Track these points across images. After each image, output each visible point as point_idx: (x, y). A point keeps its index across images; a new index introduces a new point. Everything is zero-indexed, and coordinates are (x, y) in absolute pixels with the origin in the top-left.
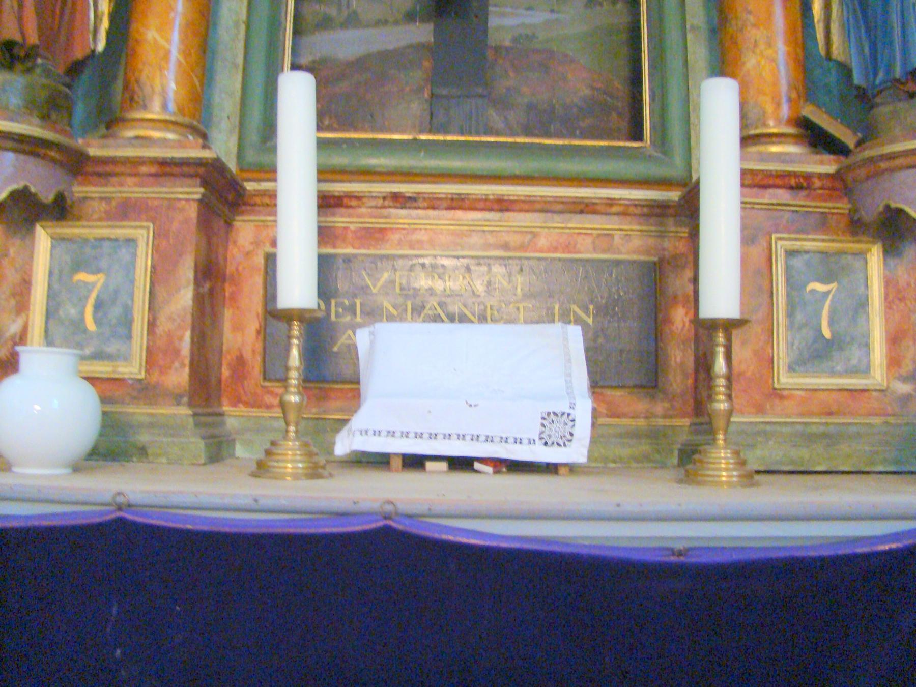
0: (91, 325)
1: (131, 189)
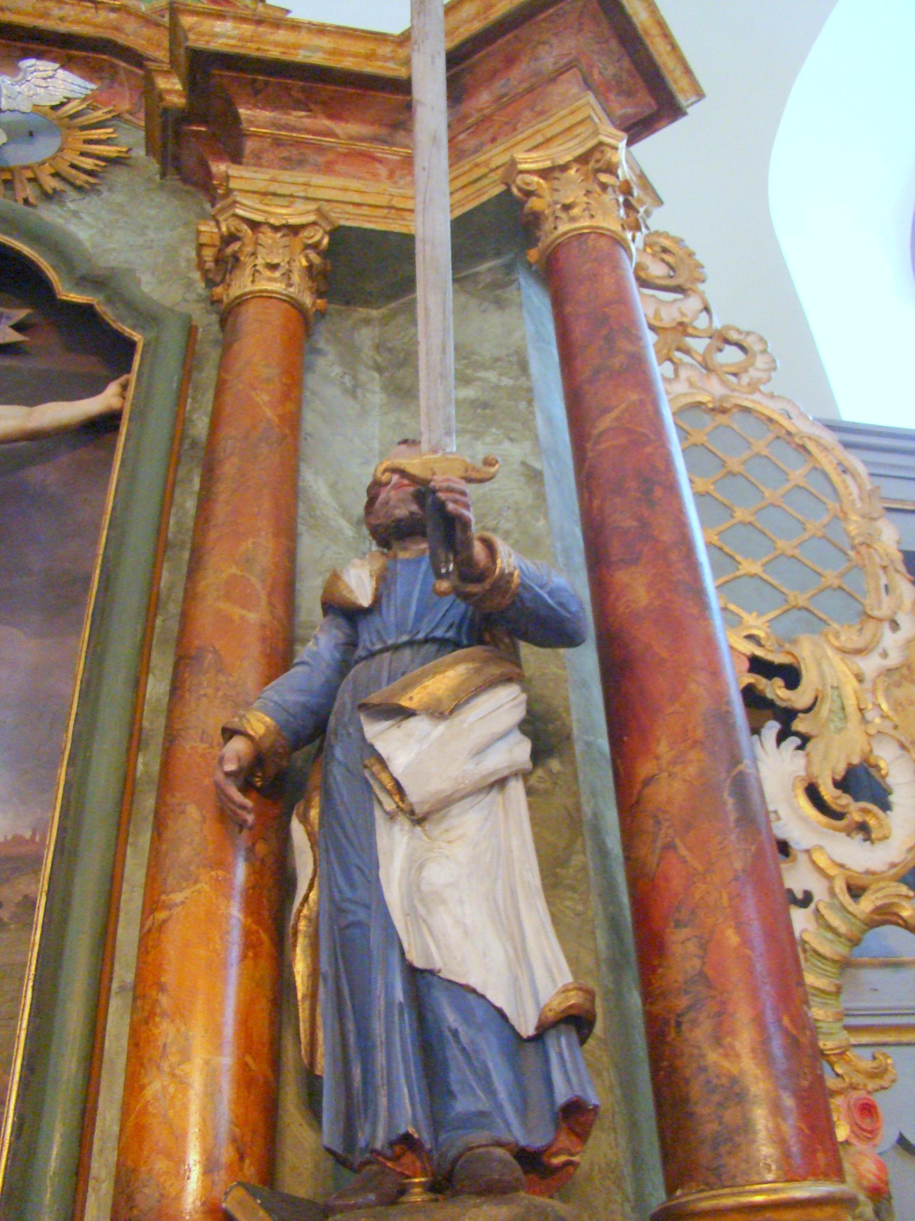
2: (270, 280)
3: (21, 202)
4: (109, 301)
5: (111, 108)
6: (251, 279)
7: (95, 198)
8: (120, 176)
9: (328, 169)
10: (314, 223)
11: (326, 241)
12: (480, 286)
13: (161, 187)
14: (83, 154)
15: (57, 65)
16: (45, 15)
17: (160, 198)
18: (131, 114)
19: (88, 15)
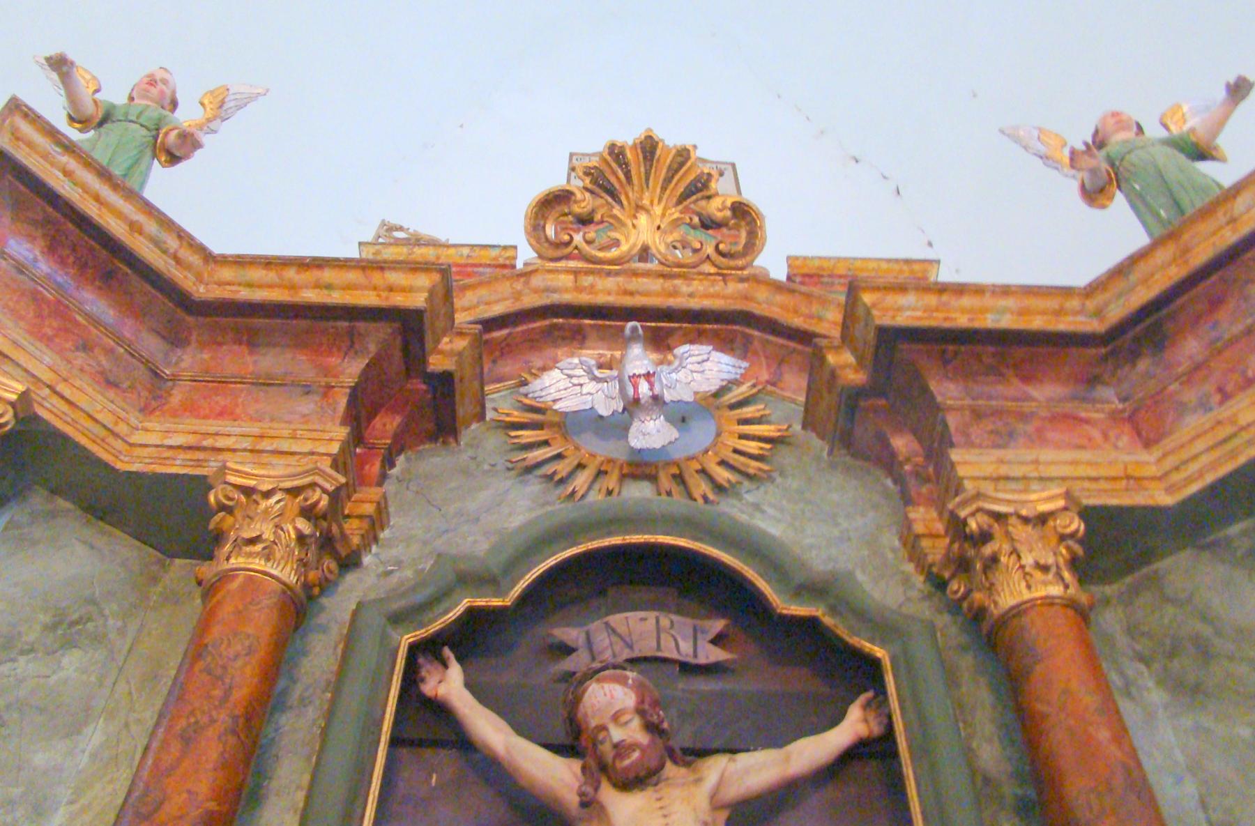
2: (1045, 583)
3: (700, 501)
4: (833, 610)
5: (753, 381)
6: (1023, 584)
7: (771, 488)
8: (786, 457)
9: (1039, 439)
10: (1065, 509)
11: (1082, 527)
12: (1239, 554)
13: (833, 466)
14: (743, 437)
15: (710, 348)
16: (675, 293)
17: (837, 478)
18: (774, 384)
19: (717, 288)
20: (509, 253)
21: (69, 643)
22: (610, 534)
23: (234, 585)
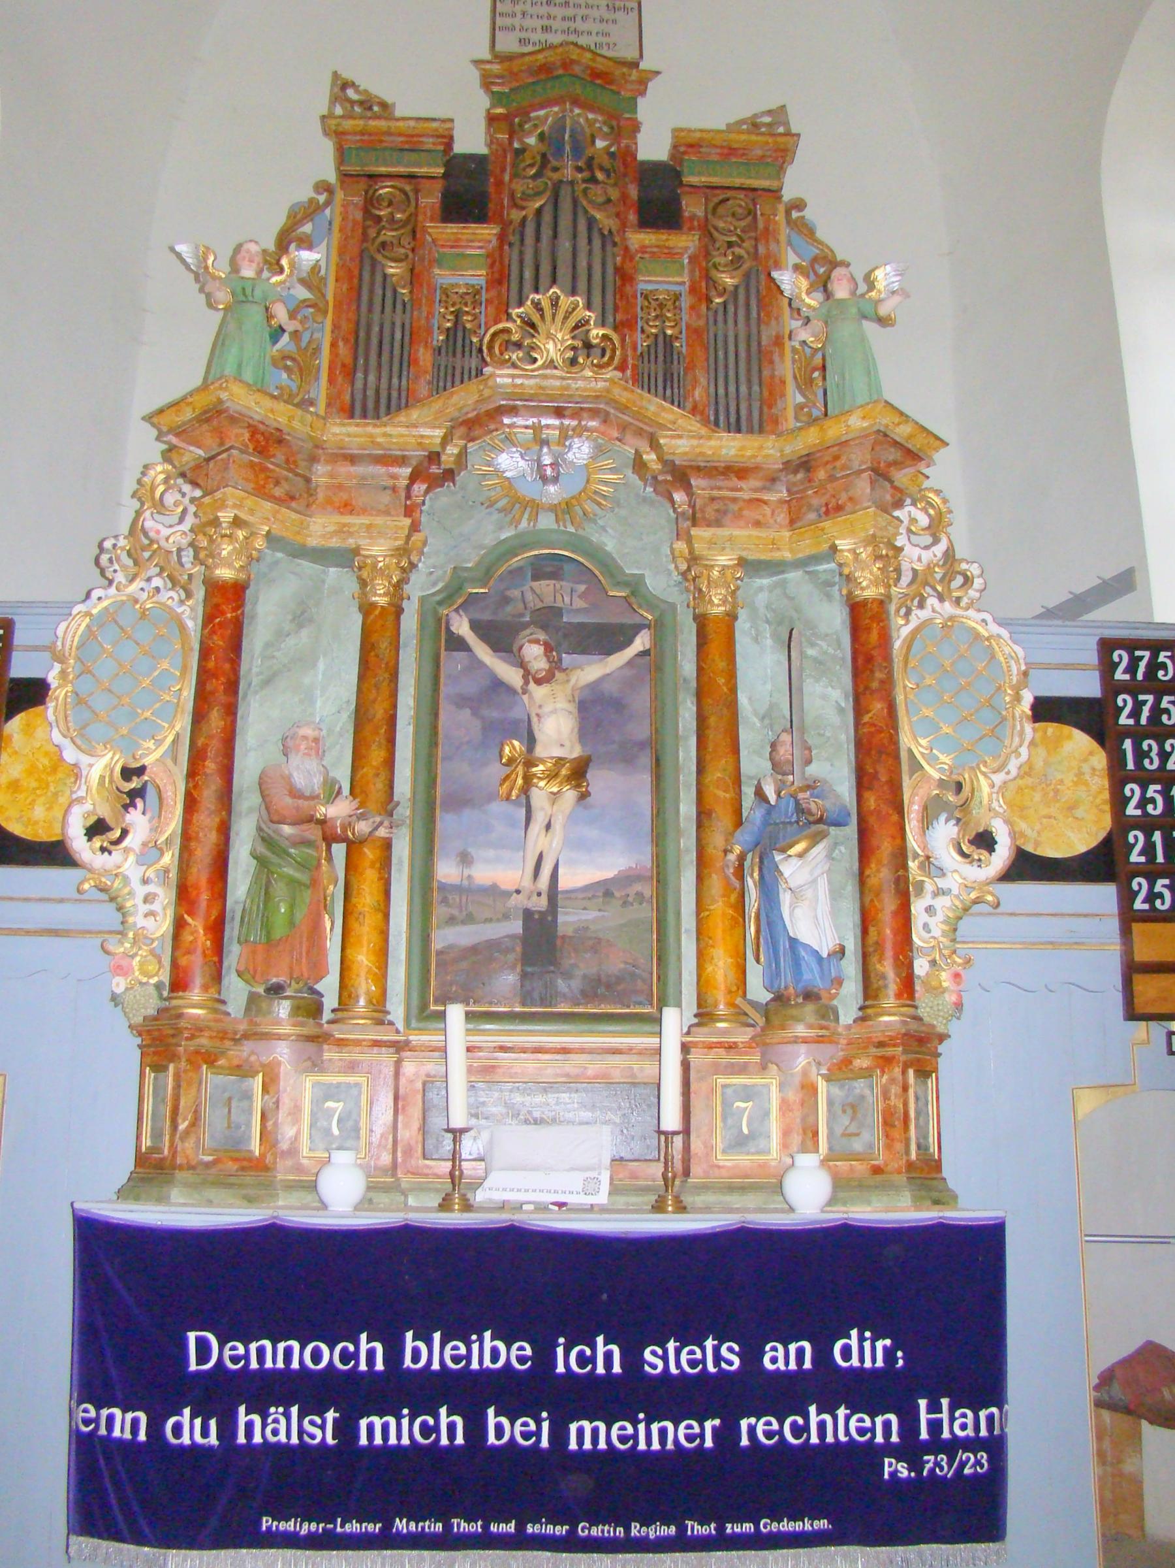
0: (336, 1132)
1: (355, 1055)
20: (448, 125)
21: (301, 626)
22: (532, 549)
23: (377, 612)
